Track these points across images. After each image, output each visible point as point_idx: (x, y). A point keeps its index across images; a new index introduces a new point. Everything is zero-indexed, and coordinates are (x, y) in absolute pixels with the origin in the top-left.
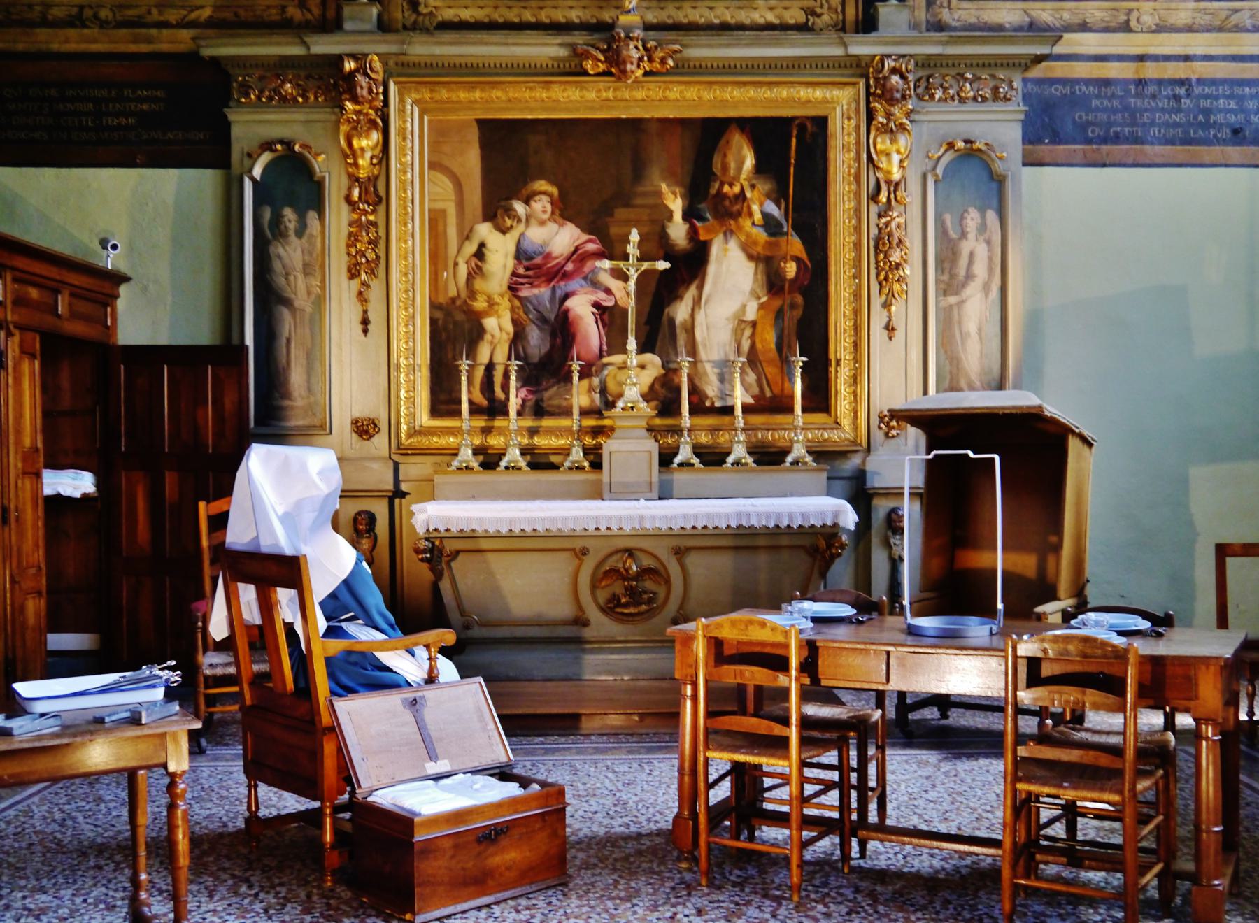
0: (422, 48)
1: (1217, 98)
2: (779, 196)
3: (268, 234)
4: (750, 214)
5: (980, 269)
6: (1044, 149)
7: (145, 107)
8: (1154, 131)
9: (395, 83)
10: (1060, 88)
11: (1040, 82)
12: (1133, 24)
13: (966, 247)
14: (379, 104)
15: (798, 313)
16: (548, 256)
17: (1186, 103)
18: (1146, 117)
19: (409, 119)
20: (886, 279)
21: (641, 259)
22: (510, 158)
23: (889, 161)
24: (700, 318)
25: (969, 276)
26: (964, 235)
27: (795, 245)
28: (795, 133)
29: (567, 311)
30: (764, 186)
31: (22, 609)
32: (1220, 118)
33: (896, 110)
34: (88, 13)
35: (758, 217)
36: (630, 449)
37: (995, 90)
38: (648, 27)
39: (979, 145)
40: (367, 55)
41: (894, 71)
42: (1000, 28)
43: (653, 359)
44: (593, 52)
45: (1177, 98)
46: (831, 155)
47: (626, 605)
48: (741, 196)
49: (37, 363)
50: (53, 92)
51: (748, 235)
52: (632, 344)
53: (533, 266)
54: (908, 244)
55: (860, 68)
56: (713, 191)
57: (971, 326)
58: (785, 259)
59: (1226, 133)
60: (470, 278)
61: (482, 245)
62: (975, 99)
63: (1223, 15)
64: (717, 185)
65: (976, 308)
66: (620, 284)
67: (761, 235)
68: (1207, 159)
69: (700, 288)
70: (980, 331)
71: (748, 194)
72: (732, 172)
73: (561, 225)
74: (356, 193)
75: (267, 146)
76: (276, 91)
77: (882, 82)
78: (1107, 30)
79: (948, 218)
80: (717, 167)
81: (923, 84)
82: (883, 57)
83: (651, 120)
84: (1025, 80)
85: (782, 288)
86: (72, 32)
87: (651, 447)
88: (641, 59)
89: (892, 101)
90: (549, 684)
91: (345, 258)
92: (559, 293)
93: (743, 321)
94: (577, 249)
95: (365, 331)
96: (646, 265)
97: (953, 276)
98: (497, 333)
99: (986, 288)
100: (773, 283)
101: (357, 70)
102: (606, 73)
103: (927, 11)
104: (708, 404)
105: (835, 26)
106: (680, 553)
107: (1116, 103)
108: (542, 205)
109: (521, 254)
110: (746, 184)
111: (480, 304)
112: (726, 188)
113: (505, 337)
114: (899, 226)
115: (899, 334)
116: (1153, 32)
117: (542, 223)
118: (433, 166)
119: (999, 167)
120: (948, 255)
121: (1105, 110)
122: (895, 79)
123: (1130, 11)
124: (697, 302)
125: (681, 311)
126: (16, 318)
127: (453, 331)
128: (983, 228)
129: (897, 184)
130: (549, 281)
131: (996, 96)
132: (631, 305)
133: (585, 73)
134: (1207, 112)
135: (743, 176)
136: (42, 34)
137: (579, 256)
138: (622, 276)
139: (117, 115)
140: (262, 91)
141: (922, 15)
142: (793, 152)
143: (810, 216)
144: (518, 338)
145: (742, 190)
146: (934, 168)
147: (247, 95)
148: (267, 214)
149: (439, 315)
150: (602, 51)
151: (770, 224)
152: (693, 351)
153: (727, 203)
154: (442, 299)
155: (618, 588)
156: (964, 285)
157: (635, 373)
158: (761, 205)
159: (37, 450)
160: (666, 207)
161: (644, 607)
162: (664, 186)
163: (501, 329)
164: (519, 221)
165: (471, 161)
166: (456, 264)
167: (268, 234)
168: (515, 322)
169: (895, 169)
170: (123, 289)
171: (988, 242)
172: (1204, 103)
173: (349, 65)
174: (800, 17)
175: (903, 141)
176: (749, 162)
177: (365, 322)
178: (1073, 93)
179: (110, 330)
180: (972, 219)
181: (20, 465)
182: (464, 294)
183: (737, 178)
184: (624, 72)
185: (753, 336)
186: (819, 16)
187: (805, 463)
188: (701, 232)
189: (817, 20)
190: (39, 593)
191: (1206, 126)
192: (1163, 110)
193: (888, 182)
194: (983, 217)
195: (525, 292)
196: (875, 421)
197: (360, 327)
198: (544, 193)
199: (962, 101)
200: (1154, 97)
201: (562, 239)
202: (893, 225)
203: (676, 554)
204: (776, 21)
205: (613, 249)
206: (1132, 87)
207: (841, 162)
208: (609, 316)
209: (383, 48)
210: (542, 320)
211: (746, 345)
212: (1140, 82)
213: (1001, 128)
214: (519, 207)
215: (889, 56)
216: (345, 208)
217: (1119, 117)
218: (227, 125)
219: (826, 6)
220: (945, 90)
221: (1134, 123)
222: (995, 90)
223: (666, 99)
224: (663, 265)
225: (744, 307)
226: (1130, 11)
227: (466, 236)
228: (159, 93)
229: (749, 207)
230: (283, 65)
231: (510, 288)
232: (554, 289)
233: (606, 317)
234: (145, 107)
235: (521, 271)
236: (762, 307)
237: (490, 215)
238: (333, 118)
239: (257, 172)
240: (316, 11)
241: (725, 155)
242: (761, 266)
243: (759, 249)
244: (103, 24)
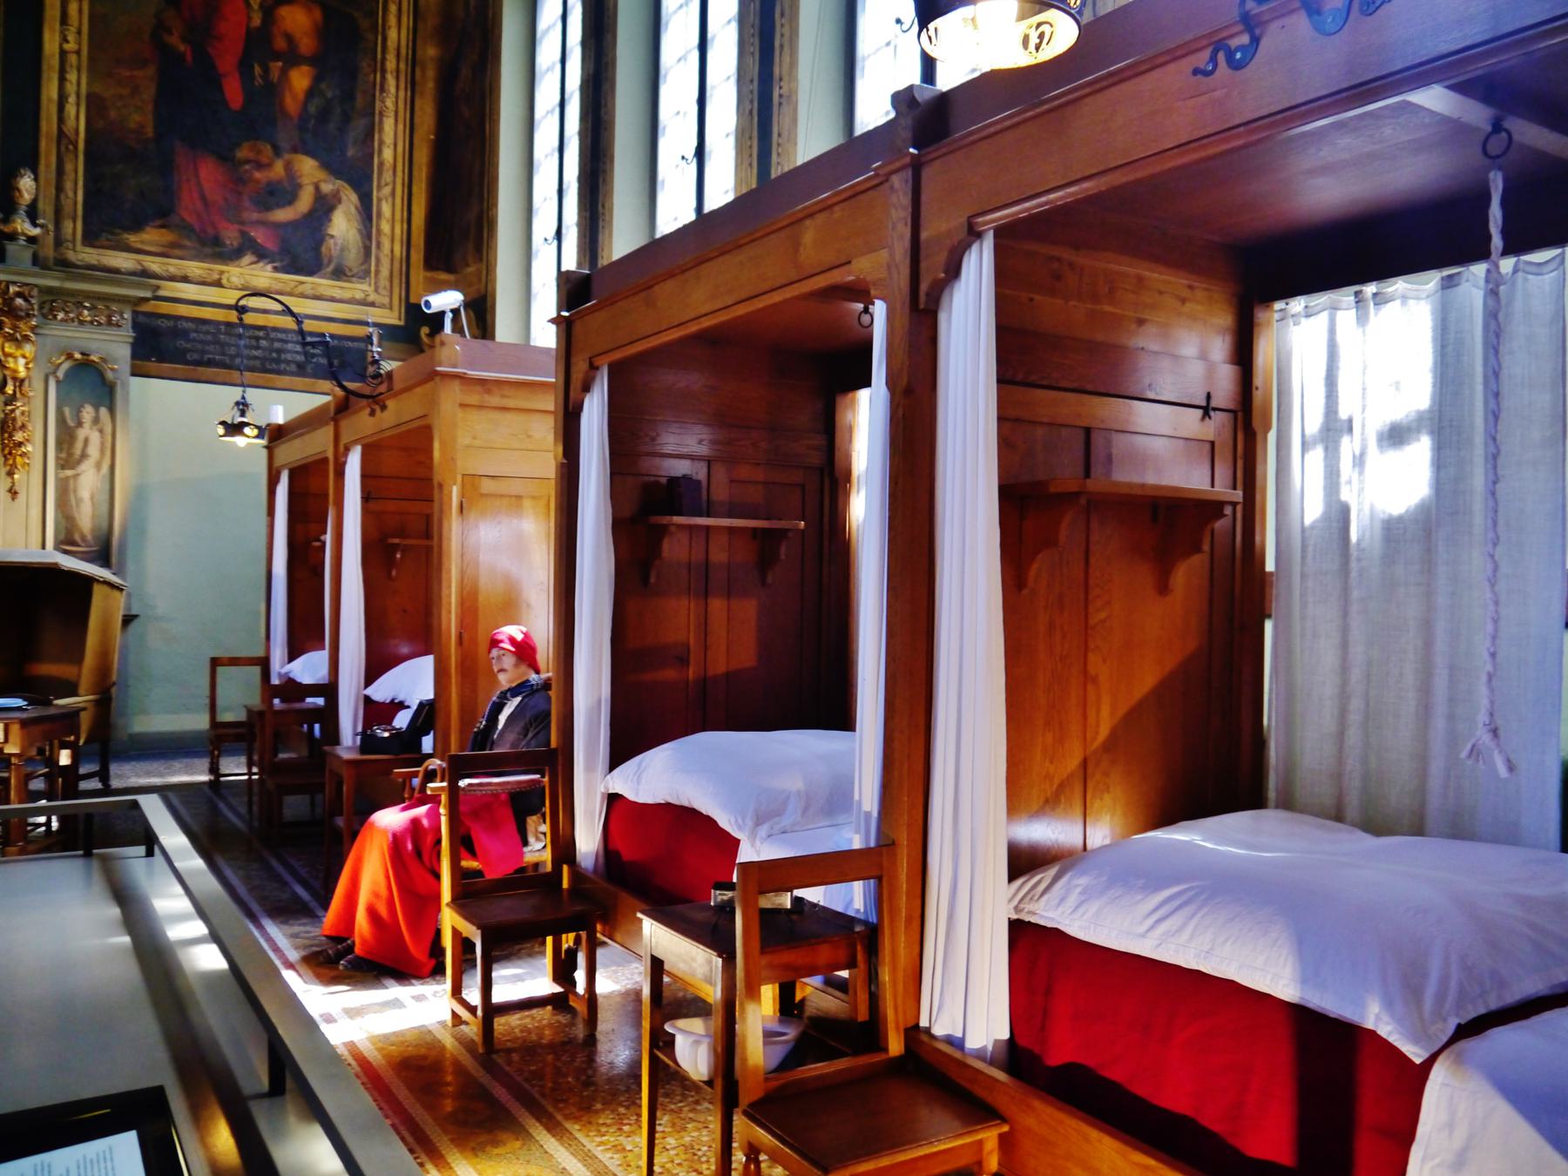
1: (286, 342)
5: (93, 450)
6: (152, 365)
8: (238, 361)
12: (224, 282)
13: (81, 434)
17: (264, 343)
18: (233, 351)
25: (84, 456)
26: (80, 424)
32: (289, 357)
33: (22, 325)
37: (109, 317)
39: (93, 358)
41: (19, 295)
42: (117, 271)
45: (257, 339)
59: (293, 368)
63: (293, 284)
65: (88, 480)
68: (279, 384)
70: (92, 498)
79: (67, 411)
81: (47, 306)
82: (8, 283)
84: (135, 313)
89: (20, 318)
97: (70, 455)
99: (98, 466)
115: (22, 497)
119: (110, 375)
120: (66, 436)
121: (201, 342)
122: (19, 301)
123: (222, 273)
128: (96, 420)
131: (109, 323)
134: (279, 351)
141: (48, 251)
146: (54, 373)
156: (79, 462)
169: (21, 369)
171: (101, 431)
172: (277, 345)
175: (28, 349)
180: (88, 413)
191: (278, 361)
193: (15, 379)
194: (97, 411)
199: (82, 323)
202: (18, 412)
213: (114, 347)
215: (14, 283)
217: (211, 348)
221: (223, 354)
222: (109, 317)
226: (222, 273)
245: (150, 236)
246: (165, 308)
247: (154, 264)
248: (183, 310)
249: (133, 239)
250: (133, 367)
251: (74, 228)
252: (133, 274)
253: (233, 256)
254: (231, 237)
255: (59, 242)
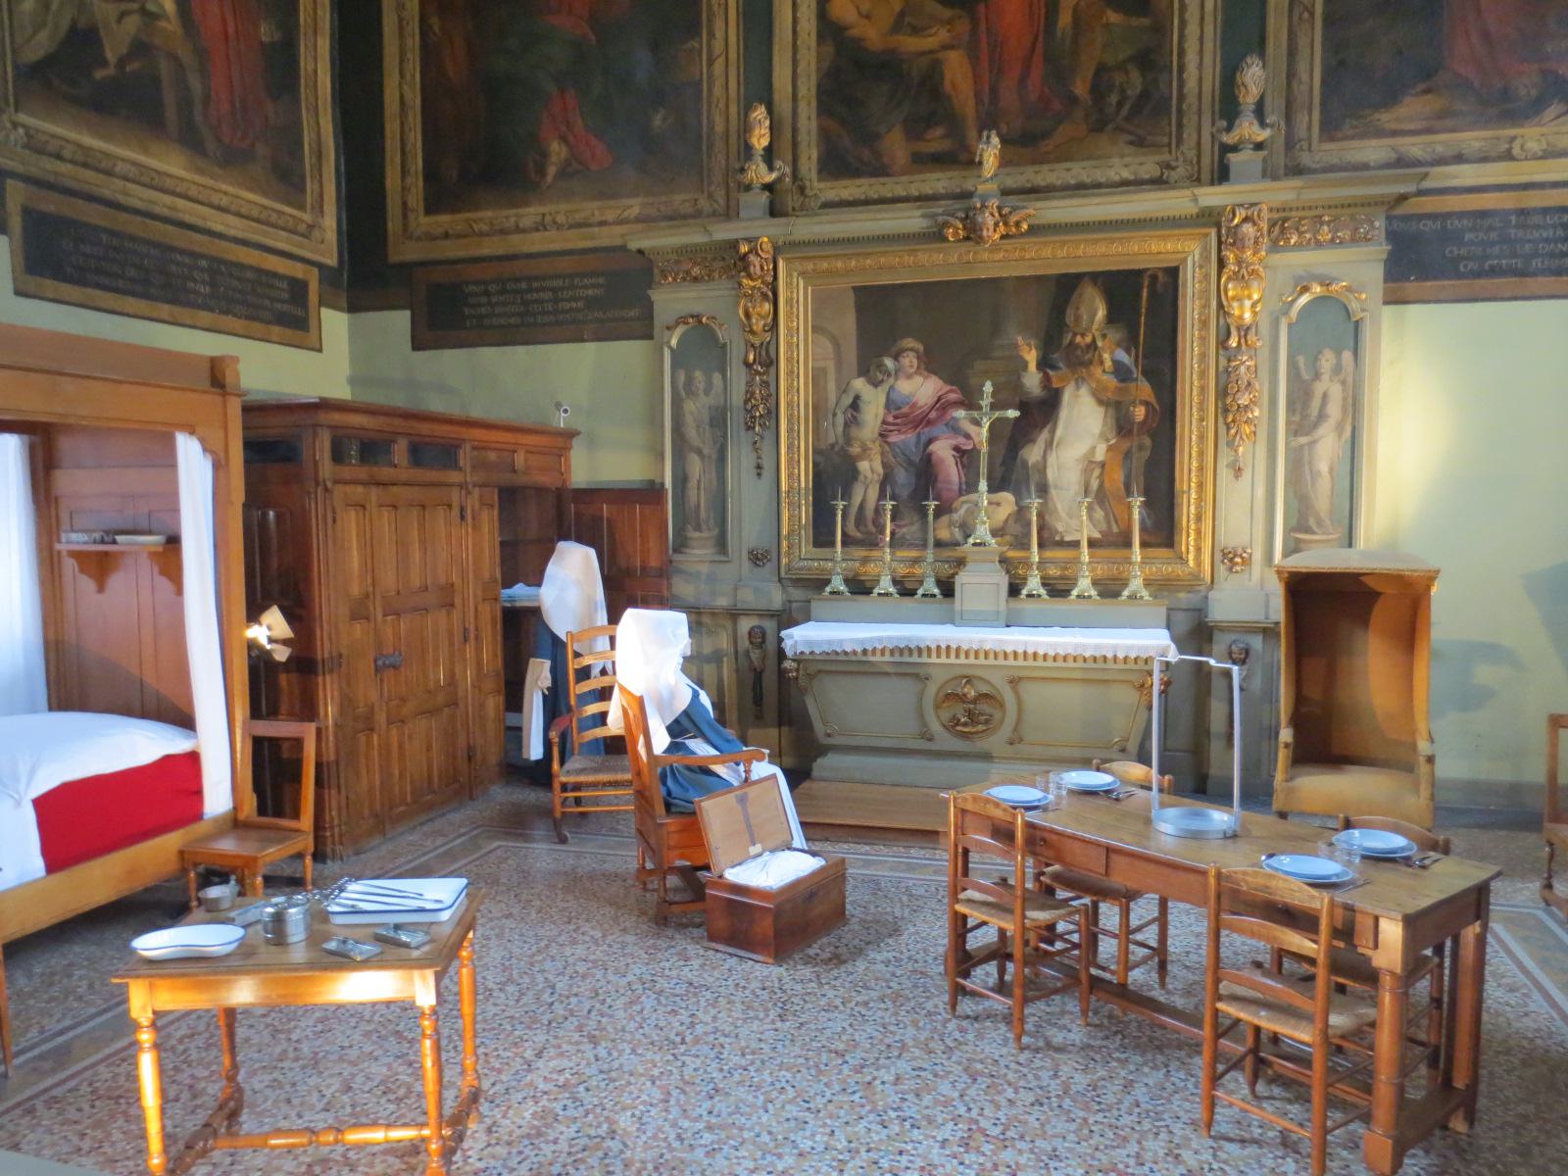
0: (805, 228)
2: (1130, 342)
3: (683, 393)
4: (1102, 363)
5: (1334, 410)
6: (1411, 287)
7: (590, 292)
9: (786, 260)
10: (1430, 223)
11: (1407, 218)
12: (1516, 151)
13: (1319, 388)
14: (770, 279)
15: (1147, 454)
16: (914, 406)
19: (796, 294)
20: (1233, 421)
21: (994, 407)
22: (882, 319)
23: (1241, 307)
24: (1052, 460)
25: (1322, 416)
26: (1317, 376)
27: (1144, 389)
28: (1146, 283)
29: (930, 455)
30: (1115, 335)
31: (482, 706)
34: (548, 219)
35: (1108, 364)
36: (980, 583)
38: (1006, 192)
40: (757, 238)
41: (1246, 220)
42: (1365, 167)
43: (1007, 498)
44: (951, 220)
46: (1180, 303)
47: (965, 725)
48: (1093, 346)
49: (496, 512)
50: (524, 285)
51: (1098, 381)
52: (983, 485)
53: (901, 415)
54: (1257, 386)
55: (1210, 218)
56: (1067, 340)
57: (1323, 467)
58: (1133, 403)
60: (847, 425)
61: (857, 398)
62: (1332, 240)
64: (1070, 336)
66: (976, 428)
67: (1111, 381)
69: (1053, 431)
70: (1331, 470)
71: (1100, 344)
72: (1084, 324)
73: (926, 378)
74: (751, 357)
75: (682, 320)
76: (688, 272)
77: (1234, 231)
78: (1484, 159)
79: (1301, 360)
80: (1070, 318)
83: (1007, 278)
84: (1389, 218)
85: (1130, 432)
86: (537, 236)
87: (1003, 581)
88: (996, 225)
90: (898, 789)
91: (742, 413)
92: (924, 439)
93: (1091, 462)
94: (939, 400)
95: (759, 475)
96: (997, 414)
97: (1304, 417)
98: (869, 475)
99: (1339, 428)
100: (1123, 426)
101: (750, 251)
102: (967, 239)
103: (1286, 155)
104: (1057, 538)
105: (1191, 176)
106: (1014, 682)
107: (1493, 235)
108: (909, 361)
109: (890, 404)
110: (1097, 334)
111: (855, 450)
112: (1078, 339)
113: (876, 478)
114: (1248, 368)
115: (1247, 475)
116: (1541, 158)
117: (909, 377)
118: (815, 329)
123: (1513, 139)
124: (1049, 444)
125: (1032, 454)
126: (475, 479)
127: (832, 476)
128: (1337, 369)
129: (1248, 328)
130: (916, 427)
132: (984, 449)
133: (946, 239)
135: (1095, 326)
136: (515, 238)
137: (942, 405)
138: (977, 423)
139: (569, 300)
140: (677, 274)
141: (1280, 160)
142: (1145, 305)
143: (1159, 360)
144: (886, 480)
145: (1094, 341)
147: (666, 278)
148: (682, 378)
149: (820, 459)
150: (962, 220)
151: (1121, 372)
152: (1043, 490)
153: (1079, 353)
154: (823, 446)
155: (959, 710)
156: (1315, 426)
157: (989, 510)
158: (1112, 353)
159: (496, 581)
160: (1022, 358)
161: (980, 727)
162: (1020, 338)
163: (872, 471)
164: (889, 375)
165: (848, 324)
166: (835, 415)
167: (683, 393)
168: (884, 465)
169: (1247, 315)
170: (575, 442)
171: (1343, 383)
173: (744, 248)
174: (1155, 171)
176: (1101, 313)
177: (759, 467)
178: (1444, 228)
179: (563, 473)
180: (1327, 361)
181: (479, 593)
182: (841, 441)
183: (1089, 329)
184: (981, 237)
185: (1102, 474)
186: (1173, 169)
187: (1142, 597)
188: (1054, 379)
189: (1173, 173)
190: (499, 692)
192: (1547, 240)
195: (893, 438)
196: (1218, 556)
197: (755, 471)
198: (911, 349)
199: (1319, 245)
200: (1537, 227)
201: (922, 389)
202: (1243, 369)
203: (1011, 682)
204: (1132, 177)
205: (970, 403)
206: (1513, 218)
207: (1191, 309)
208: (966, 457)
209: (773, 231)
210: (910, 462)
211: (1095, 484)
212: (1522, 212)
214: (889, 363)
216: (743, 369)
217: (1496, 250)
218: (650, 305)
219: (1181, 159)
220: (1301, 234)
221: (1514, 255)
223: (1023, 259)
224: (1012, 413)
225: (1093, 449)
226: (1513, 139)
227: (843, 390)
228: (601, 280)
229: (1100, 356)
230: (690, 253)
231: (881, 435)
232: (919, 434)
233: (965, 459)
234: (590, 292)
235: (890, 419)
236: (1110, 449)
237: (864, 371)
238: (733, 292)
239: (674, 342)
240: (722, 201)
241: (1078, 308)
242: (1111, 411)
243: (1110, 395)
244: (559, 227)
245: (1413, 108)
246: (1430, 205)
247: (1414, 147)
248: (1455, 203)
249: (1386, 118)
250: (1386, 292)
251: (1309, 121)
252: (1388, 166)
253: (1533, 110)
254: (1526, 85)
255: (1290, 145)
